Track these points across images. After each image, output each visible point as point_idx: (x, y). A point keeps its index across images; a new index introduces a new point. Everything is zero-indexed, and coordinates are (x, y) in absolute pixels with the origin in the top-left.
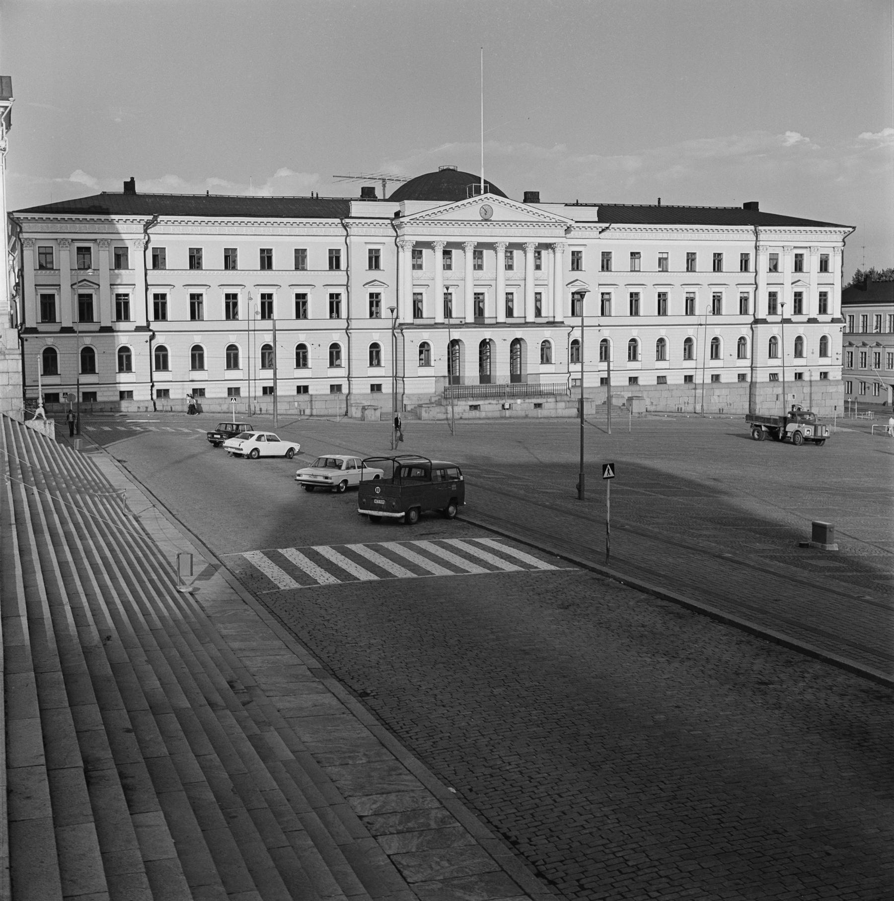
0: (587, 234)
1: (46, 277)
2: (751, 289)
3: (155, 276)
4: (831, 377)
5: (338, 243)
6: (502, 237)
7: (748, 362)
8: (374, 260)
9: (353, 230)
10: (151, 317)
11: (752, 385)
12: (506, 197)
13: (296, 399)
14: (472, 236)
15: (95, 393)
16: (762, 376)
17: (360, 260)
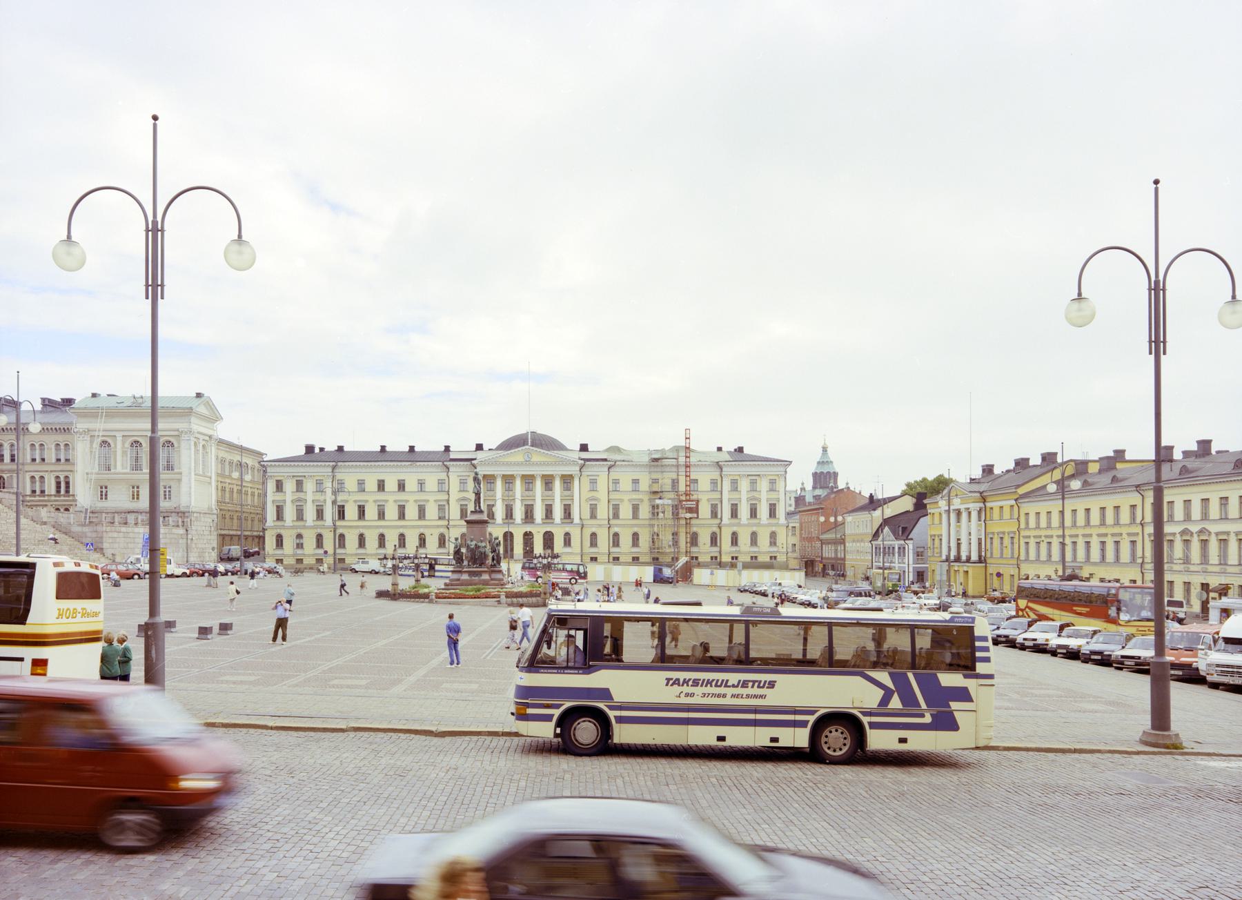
1: (279, 497)
6: (538, 471)
14: (518, 471)
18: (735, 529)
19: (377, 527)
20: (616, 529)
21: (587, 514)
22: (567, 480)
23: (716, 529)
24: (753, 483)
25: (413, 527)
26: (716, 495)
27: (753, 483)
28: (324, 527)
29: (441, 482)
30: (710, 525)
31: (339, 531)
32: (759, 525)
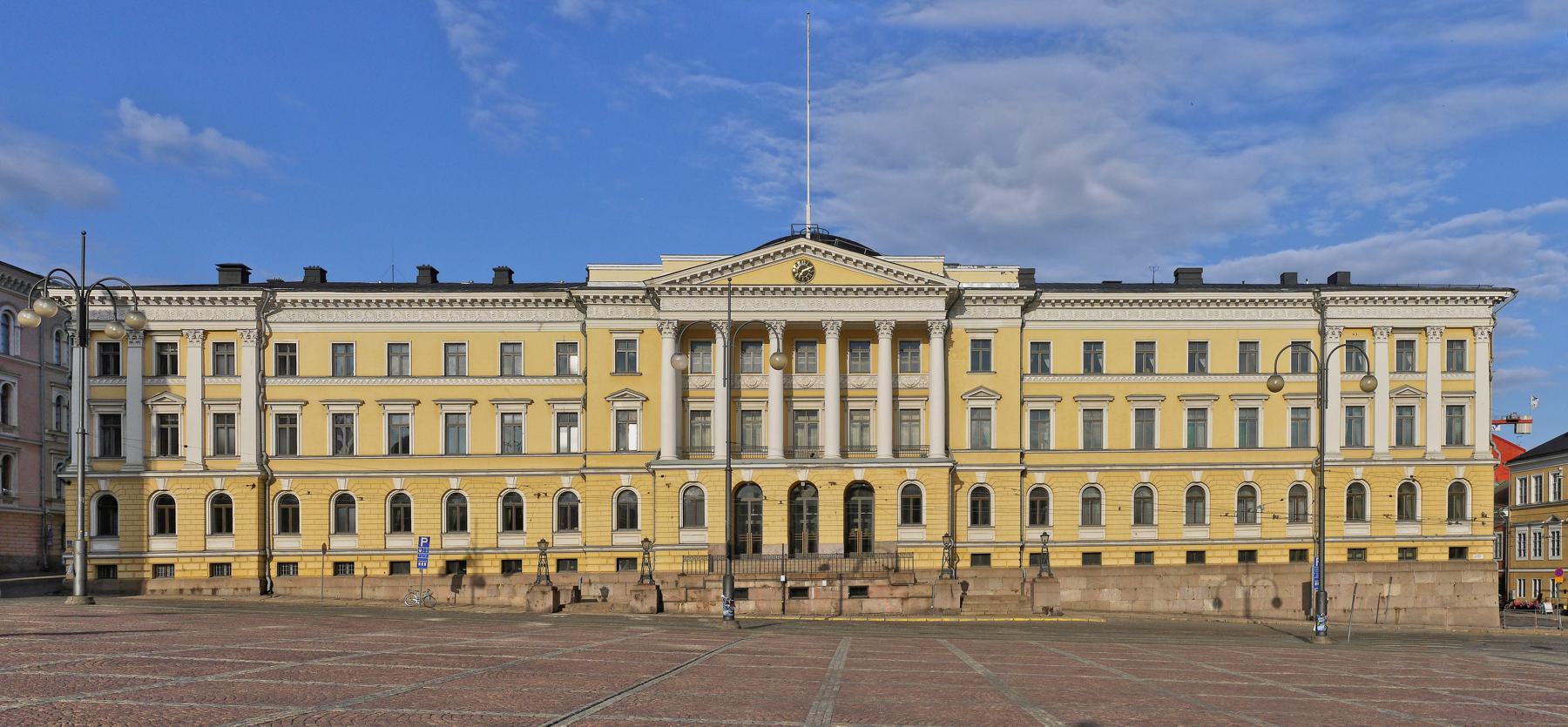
0: (1001, 311)
1: (106, 388)
2: (1313, 405)
3: (279, 388)
4: (1473, 556)
5: (571, 332)
7: (1307, 530)
8: (625, 361)
9: (593, 311)
10: (271, 449)
11: (1321, 567)
12: (871, 254)
13: (385, 583)
15: (229, 565)
16: (1335, 554)
17: (602, 356)
18: (1358, 473)
19: (388, 474)
20: (1039, 478)
21: (963, 435)
22: (909, 337)
23: (1301, 475)
24: (1405, 347)
25: (489, 473)
26: (1307, 383)
27: (1405, 347)
28: (232, 475)
29: (565, 349)
30: (1292, 466)
31: (283, 485)
32: (1370, 462)
